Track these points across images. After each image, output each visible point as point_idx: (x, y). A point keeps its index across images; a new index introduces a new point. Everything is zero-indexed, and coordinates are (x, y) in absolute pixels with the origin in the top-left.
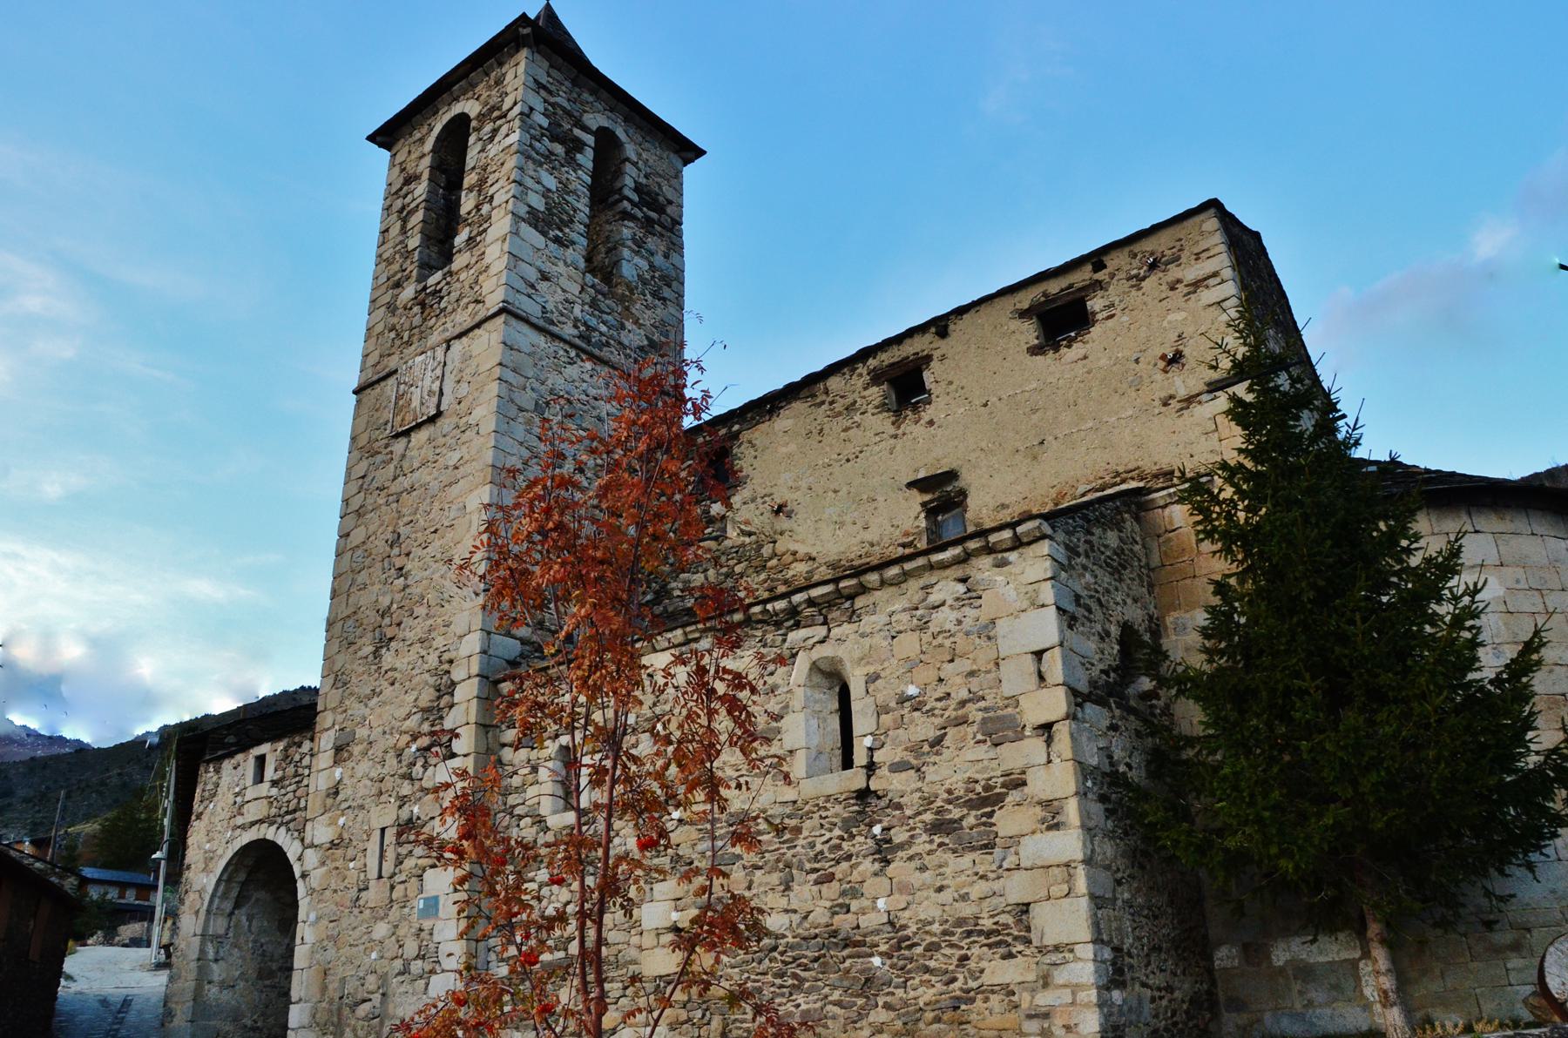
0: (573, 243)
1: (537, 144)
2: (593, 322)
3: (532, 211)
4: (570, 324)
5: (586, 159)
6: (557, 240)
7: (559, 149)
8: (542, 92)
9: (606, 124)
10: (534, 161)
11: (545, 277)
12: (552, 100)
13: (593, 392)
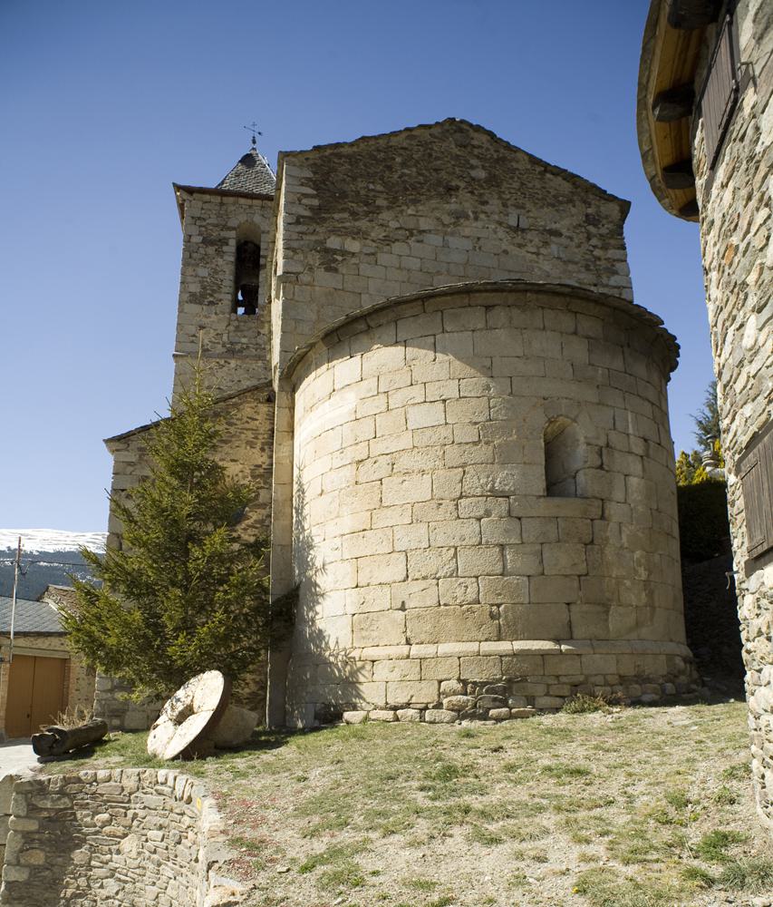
0: (221, 300)
1: (195, 255)
2: (237, 339)
3: (193, 295)
4: (220, 346)
5: (231, 248)
6: (211, 303)
7: (211, 250)
8: (198, 223)
9: (242, 218)
10: (193, 265)
11: (202, 327)
12: (204, 223)
13: (236, 379)
